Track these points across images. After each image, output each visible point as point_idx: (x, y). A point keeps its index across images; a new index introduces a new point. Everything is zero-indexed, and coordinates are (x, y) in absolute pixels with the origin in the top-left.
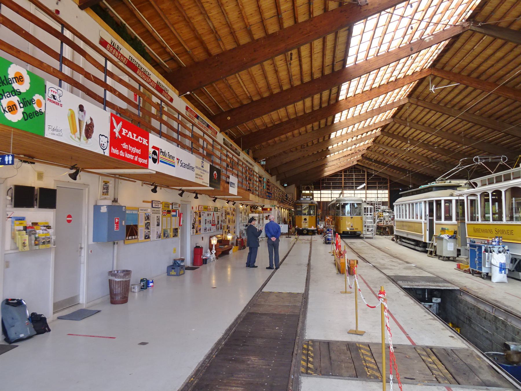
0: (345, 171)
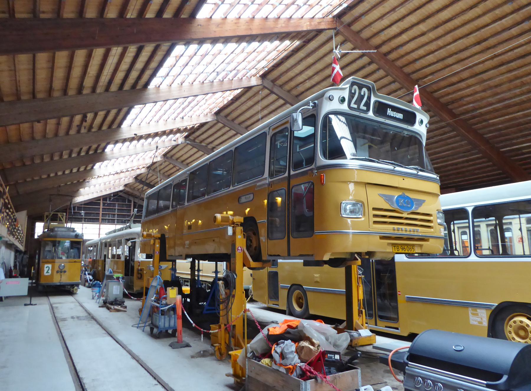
0: (105, 198)
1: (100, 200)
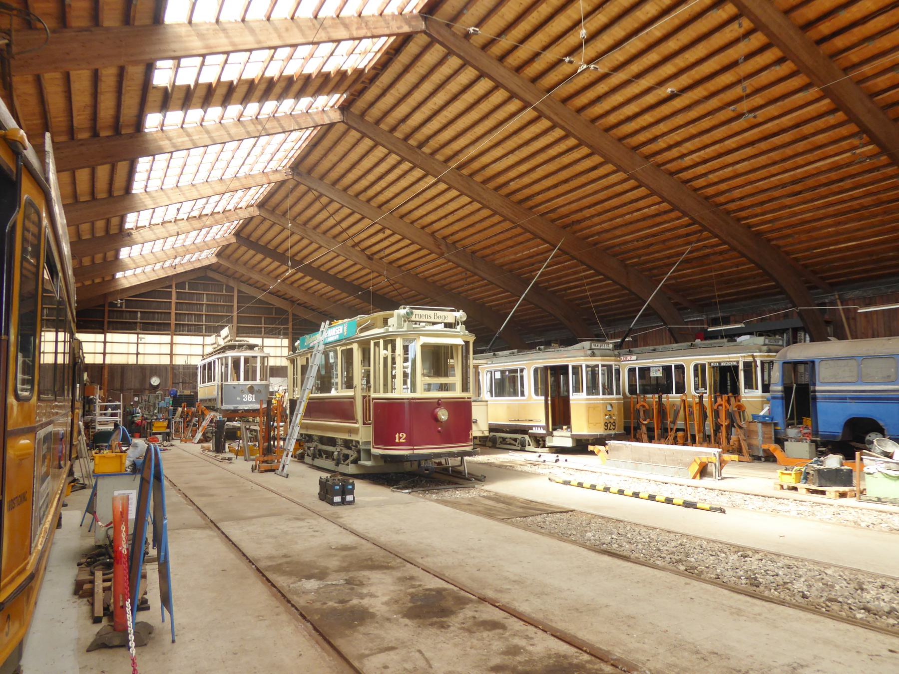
1: (170, 287)
